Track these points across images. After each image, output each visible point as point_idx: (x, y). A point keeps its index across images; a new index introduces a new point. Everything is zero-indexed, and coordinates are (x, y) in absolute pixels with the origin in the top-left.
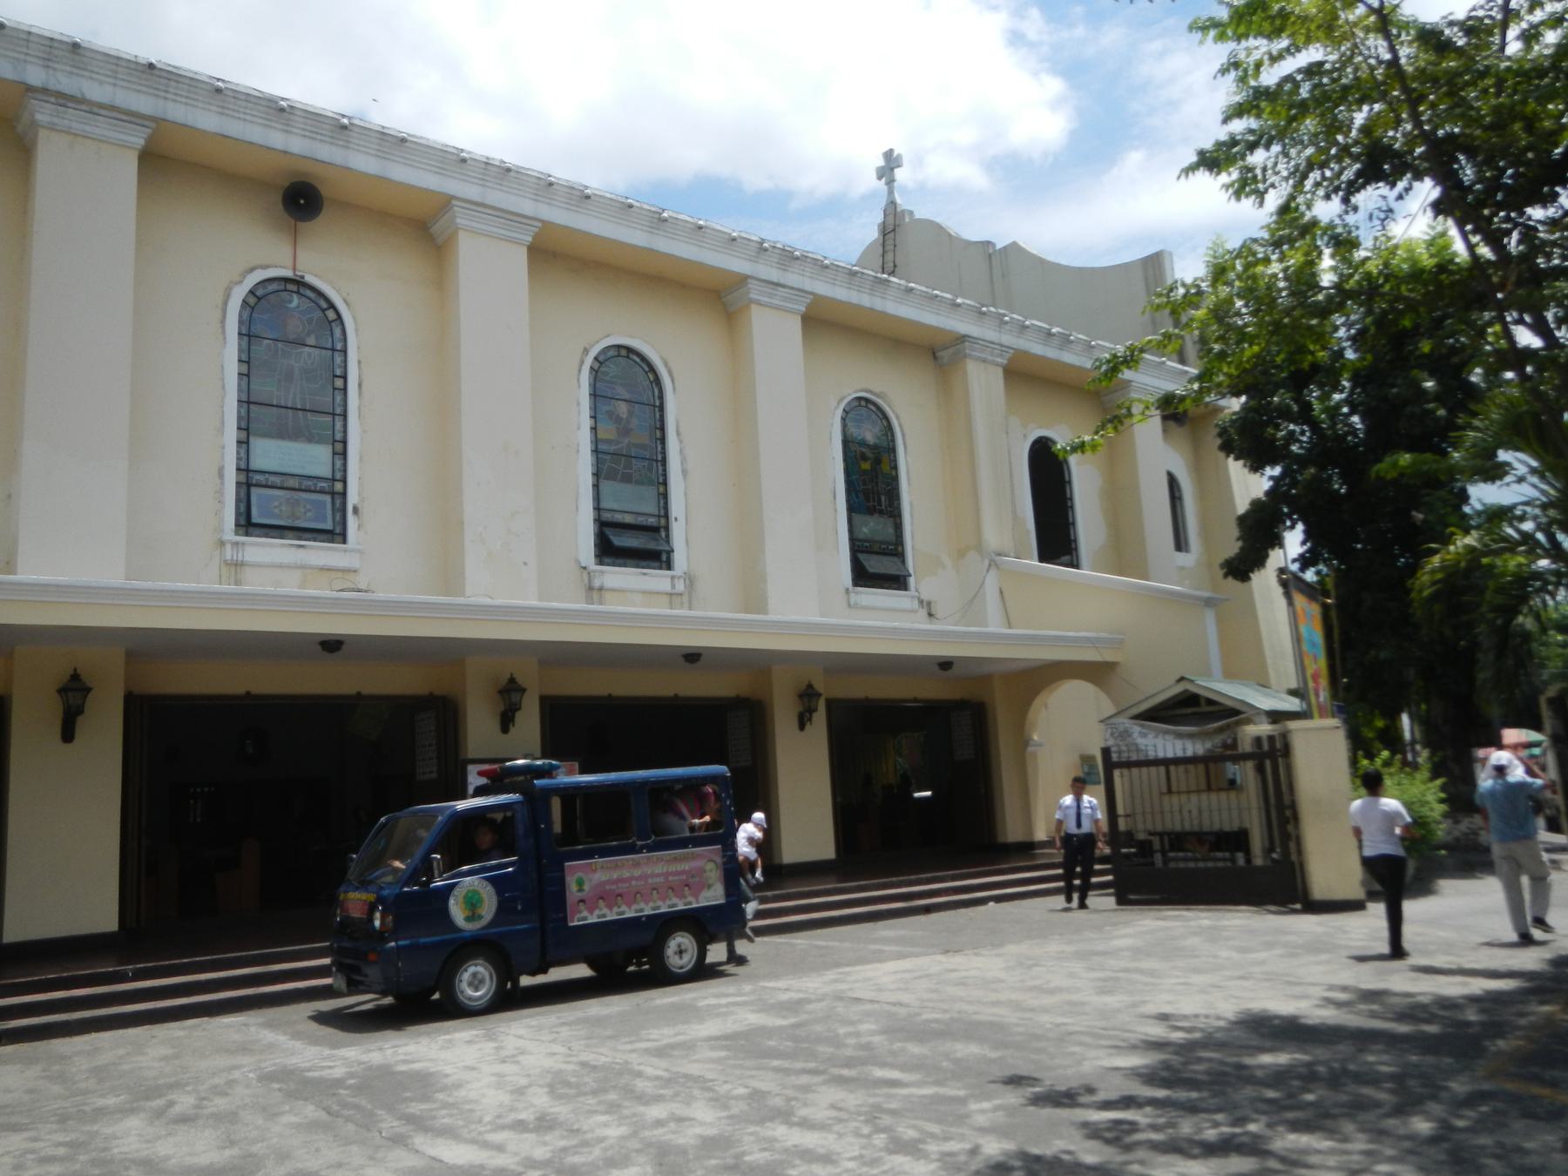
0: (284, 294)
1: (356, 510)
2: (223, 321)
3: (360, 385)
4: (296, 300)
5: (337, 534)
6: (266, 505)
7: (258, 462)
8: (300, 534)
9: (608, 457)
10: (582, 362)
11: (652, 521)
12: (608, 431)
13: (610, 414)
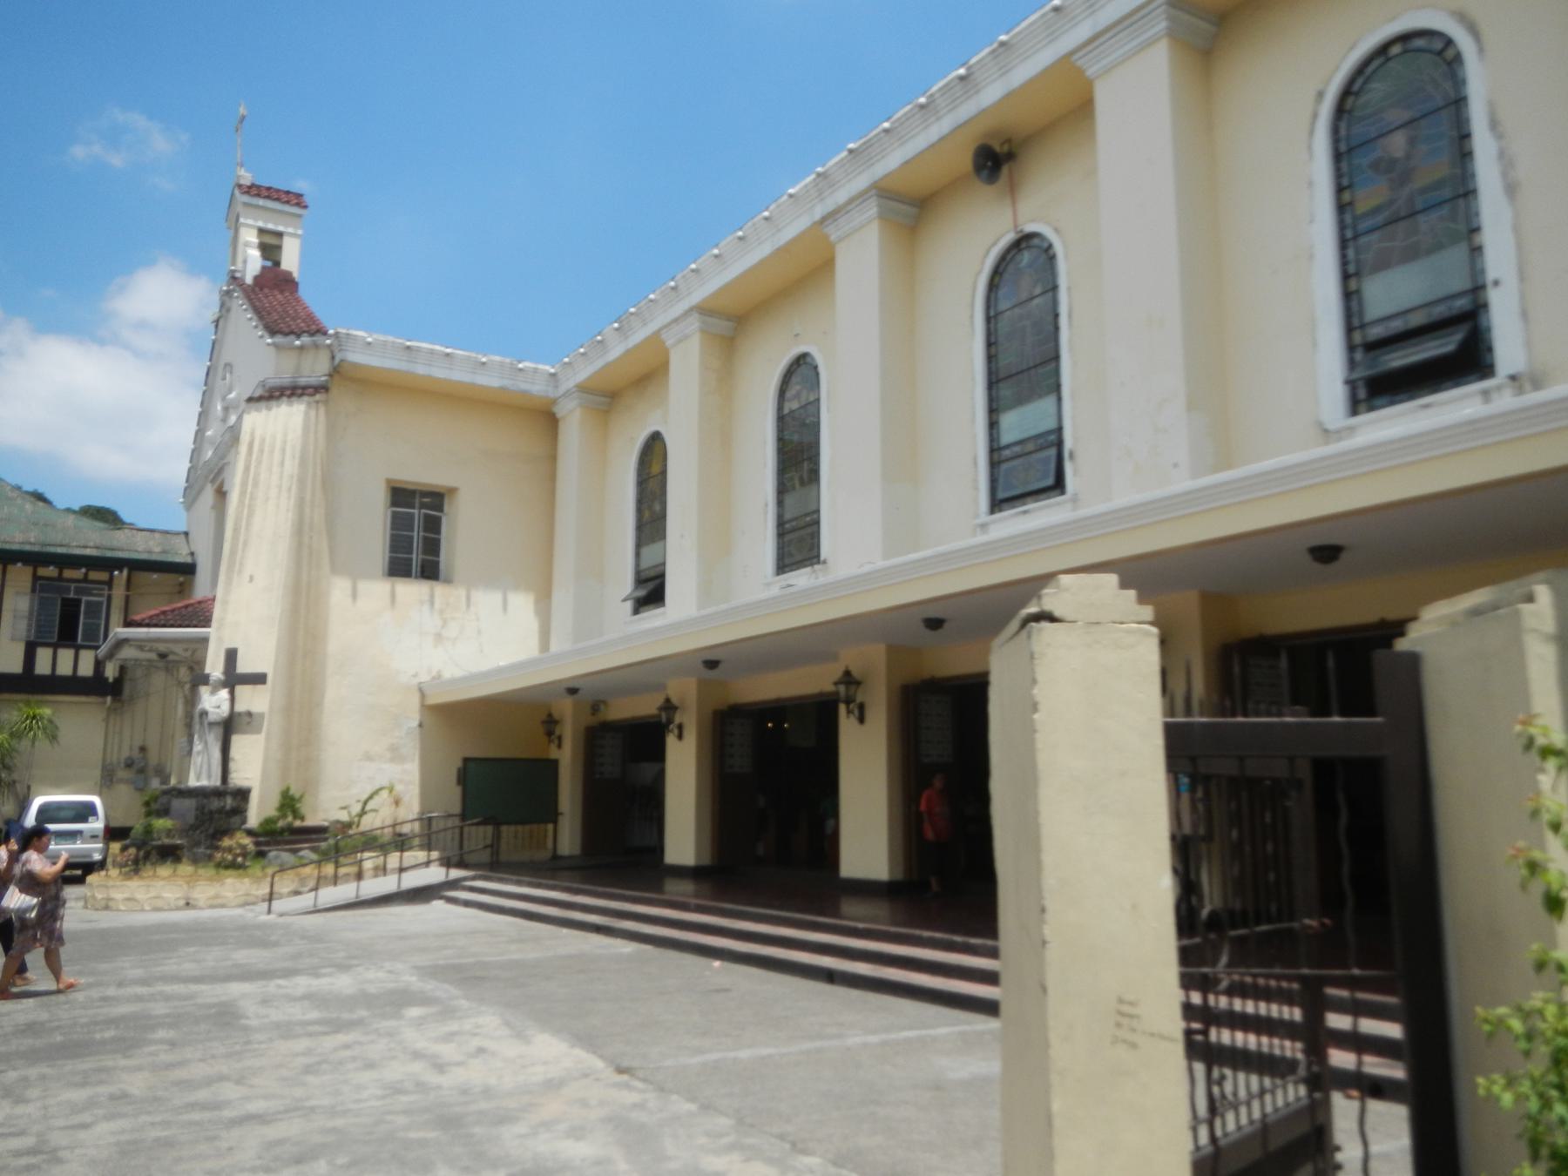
1: (1071, 456)
2: (972, 317)
5: (1059, 485)
9: (1375, 237)
10: (1315, 116)
11: (1462, 304)
12: (1370, 196)
13: (1375, 166)
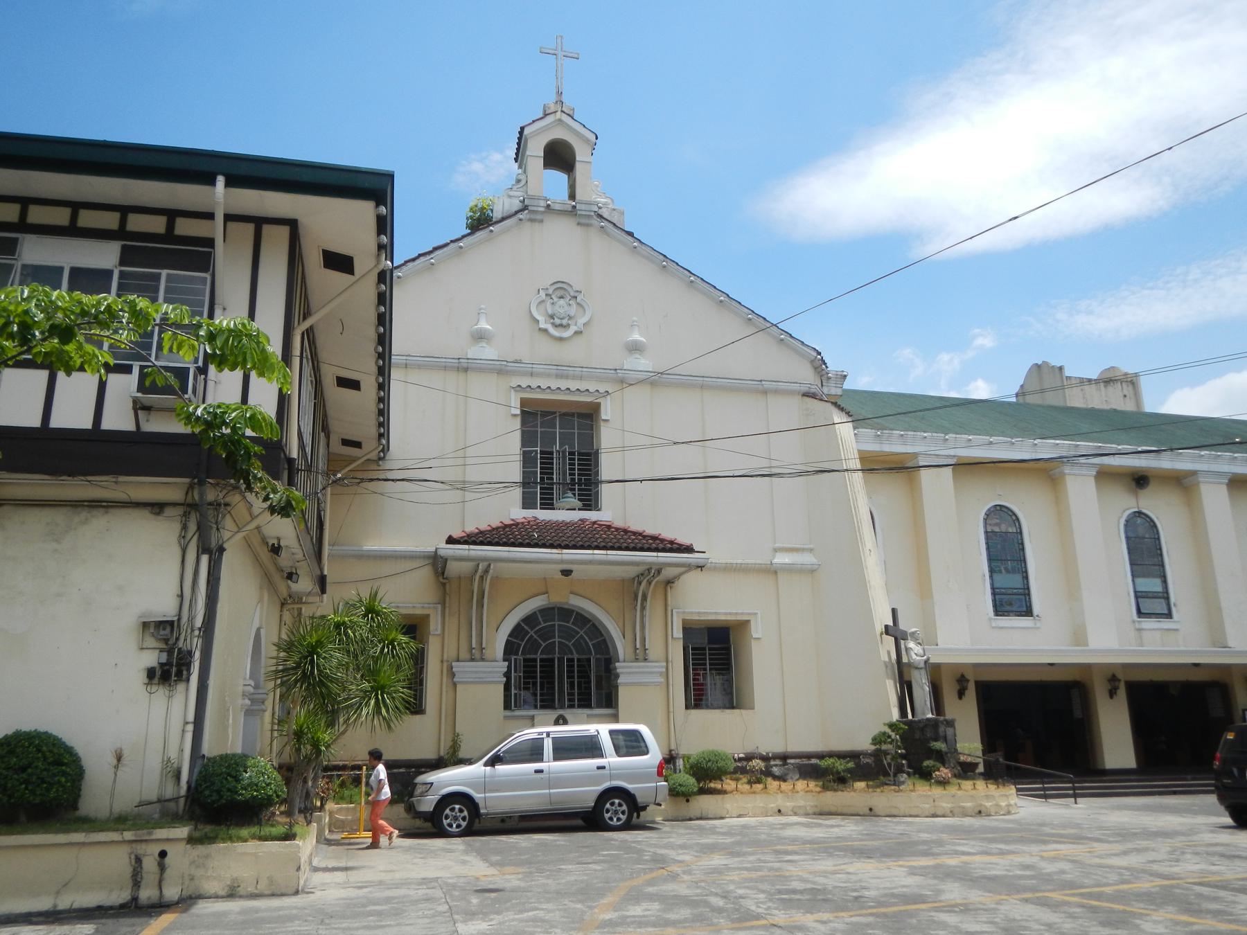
0: (1135, 518)
1: (1175, 605)
2: (1119, 534)
3: (1168, 552)
4: (1139, 519)
5: (1169, 615)
6: (1147, 605)
7: (1139, 589)
8: (1158, 616)
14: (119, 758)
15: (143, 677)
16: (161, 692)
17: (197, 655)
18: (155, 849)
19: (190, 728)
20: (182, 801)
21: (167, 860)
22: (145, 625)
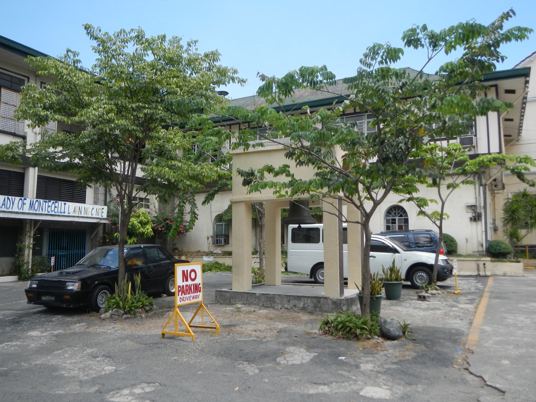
14: (467, 240)
15: (469, 220)
16: (474, 224)
17: (483, 214)
18: (483, 263)
19: (484, 233)
20: (484, 252)
21: (486, 265)
22: (468, 206)
